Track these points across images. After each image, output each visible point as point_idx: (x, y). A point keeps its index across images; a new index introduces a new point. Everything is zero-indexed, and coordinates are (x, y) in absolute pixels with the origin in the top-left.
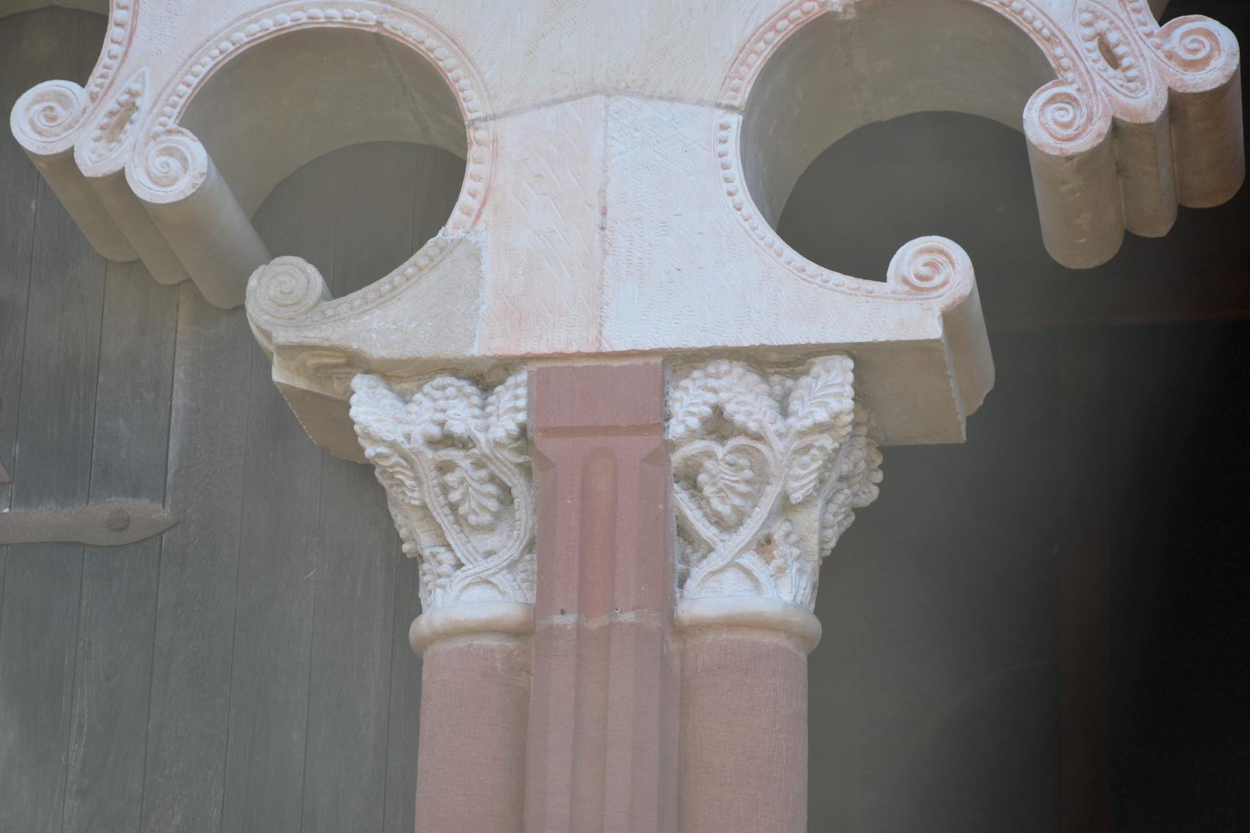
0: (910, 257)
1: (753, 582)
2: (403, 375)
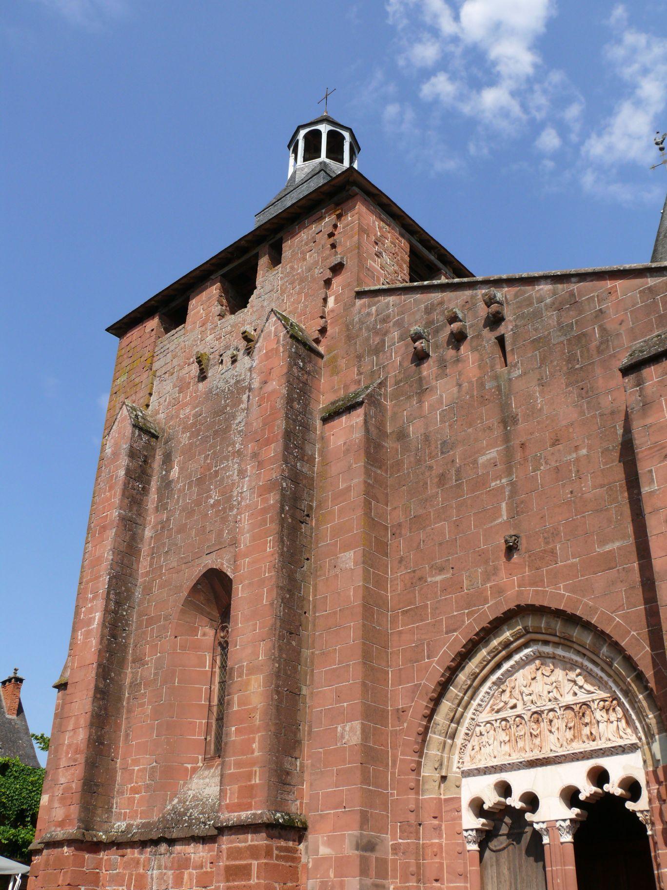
2: (537, 823)
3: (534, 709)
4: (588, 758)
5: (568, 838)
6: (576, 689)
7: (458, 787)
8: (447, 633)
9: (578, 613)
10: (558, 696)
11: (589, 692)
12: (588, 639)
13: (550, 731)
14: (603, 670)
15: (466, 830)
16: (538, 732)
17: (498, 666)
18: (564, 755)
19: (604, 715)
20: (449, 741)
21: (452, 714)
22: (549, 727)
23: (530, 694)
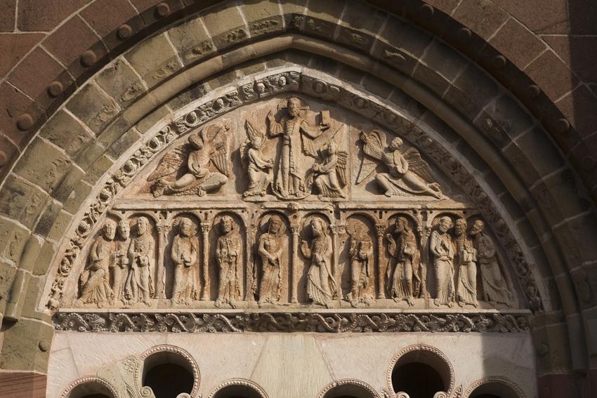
3: (270, 202)
4: (403, 330)
6: (384, 178)
7: (42, 350)
9: (453, 13)
10: (338, 188)
12: (452, 78)
13: (310, 261)
14: (465, 148)
16: (279, 254)
17: (194, 89)
18: (347, 316)
19: (449, 244)
20: (40, 239)
21: (58, 176)
22: (307, 251)
23: (266, 170)
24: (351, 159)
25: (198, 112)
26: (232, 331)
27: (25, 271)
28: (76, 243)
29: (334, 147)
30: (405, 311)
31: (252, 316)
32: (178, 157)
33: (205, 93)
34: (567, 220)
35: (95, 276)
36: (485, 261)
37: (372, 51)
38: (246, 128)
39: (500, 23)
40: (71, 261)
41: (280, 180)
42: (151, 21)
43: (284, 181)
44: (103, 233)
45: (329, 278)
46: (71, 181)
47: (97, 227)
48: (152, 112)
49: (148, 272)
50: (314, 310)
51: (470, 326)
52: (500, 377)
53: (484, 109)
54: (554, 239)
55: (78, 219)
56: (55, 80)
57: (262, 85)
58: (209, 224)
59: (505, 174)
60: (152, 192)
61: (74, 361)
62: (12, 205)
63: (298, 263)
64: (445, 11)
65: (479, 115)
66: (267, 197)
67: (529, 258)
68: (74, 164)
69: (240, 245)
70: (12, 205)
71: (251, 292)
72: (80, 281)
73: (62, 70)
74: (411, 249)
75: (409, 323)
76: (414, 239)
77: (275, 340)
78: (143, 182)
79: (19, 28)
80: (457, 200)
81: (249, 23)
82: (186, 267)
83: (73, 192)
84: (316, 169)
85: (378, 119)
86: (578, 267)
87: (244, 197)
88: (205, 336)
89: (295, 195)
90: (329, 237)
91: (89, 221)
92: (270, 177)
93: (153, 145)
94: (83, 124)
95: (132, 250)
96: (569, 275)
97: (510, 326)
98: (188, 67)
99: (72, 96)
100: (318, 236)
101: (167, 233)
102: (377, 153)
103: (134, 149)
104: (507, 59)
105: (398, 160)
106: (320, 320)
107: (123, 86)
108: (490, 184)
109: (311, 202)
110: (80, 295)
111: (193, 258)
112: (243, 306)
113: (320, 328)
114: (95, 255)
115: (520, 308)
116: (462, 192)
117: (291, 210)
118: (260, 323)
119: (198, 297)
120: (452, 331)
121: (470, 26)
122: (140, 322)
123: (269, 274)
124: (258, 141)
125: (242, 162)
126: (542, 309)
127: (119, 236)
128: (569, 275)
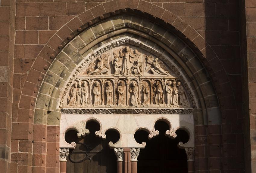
0: (143, 143)
1: (135, 159)
2: (117, 148)
3: (121, 77)
5: (136, 160)
6: (153, 70)
7: (58, 119)
8: (68, 14)
9: (172, 24)
10: (140, 72)
11: (162, 73)
12: (172, 42)
13: (132, 94)
14: (176, 61)
15: (62, 148)
17: (99, 44)
18: (142, 110)
20: (57, 88)
21: (61, 71)
22: (131, 91)
23: (120, 67)
24: (143, 64)
25: (100, 51)
26: (110, 114)
27: (53, 98)
28: (66, 89)
29: (139, 61)
30: (158, 108)
31: (116, 110)
32: (94, 63)
33: (102, 45)
34: (203, 83)
35: (72, 98)
36: (180, 93)
37: (150, 33)
38: (114, 55)
39: (186, 27)
40: (65, 94)
41: (123, 70)
42: (87, 26)
43: (124, 71)
44: (74, 85)
45: (137, 98)
46: (65, 72)
47: (72, 84)
48: (87, 51)
49: (87, 97)
50: (133, 108)
51: (176, 112)
52: (184, 126)
53: (181, 51)
54: (200, 88)
55: (67, 82)
56: (60, 44)
57: (118, 42)
58: (104, 83)
59: (187, 69)
60: (87, 74)
61: (67, 122)
62: (49, 79)
63: (129, 94)
64: (170, 24)
65: (180, 53)
66: (120, 75)
67: (193, 93)
68: (66, 67)
69: (112, 89)
70: (49, 79)
71: (115, 103)
72: (68, 100)
73: (62, 41)
74: (160, 90)
75: (160, 111)
76: (161, 87)
77: (122, 116)
78: (85, 71)
79: (50, 29)
80: (173, 76)
81: (115, 26)
82: (97, 95)
83: (65, 75)
84: (134, 67)
85: (151, 52)
86: (206, 97)
87: (113, 75)
88: (103, 115)
89: (128, 74)
90: (137, 87)
91: (70, 83)
92: (121, 69)
93: (87, 60)
94: (68, 56)
95: (82, 91)
96: (204, 99)
97: (187, 112)
98: (97, 38)
99: (65, 48)
100: (134, 87)
101: (92, 86)
102: (151, 62)
103: (82, 62)
104: (188, 38)
105: (157, 64)
106: (135, 111)
107: (79, 45)
108: (183, 72)
109: (132, 77)
110: (68, 103)
111: (99, 93)
112: (114, 106)
113: (135, 113)
114: (72, 92)
115: (190, 107)
116: (175, 73)
117: (126, 79)
118: (118, 112)
119: (101, 104)
120: (171, 113)
121: (177, 28)
122: (85, 111)
123: (120, 97)
124: (117, 59)
125: (113, 65)
126: (196, 107)
127: (78, 87)
128: (204, 99)
